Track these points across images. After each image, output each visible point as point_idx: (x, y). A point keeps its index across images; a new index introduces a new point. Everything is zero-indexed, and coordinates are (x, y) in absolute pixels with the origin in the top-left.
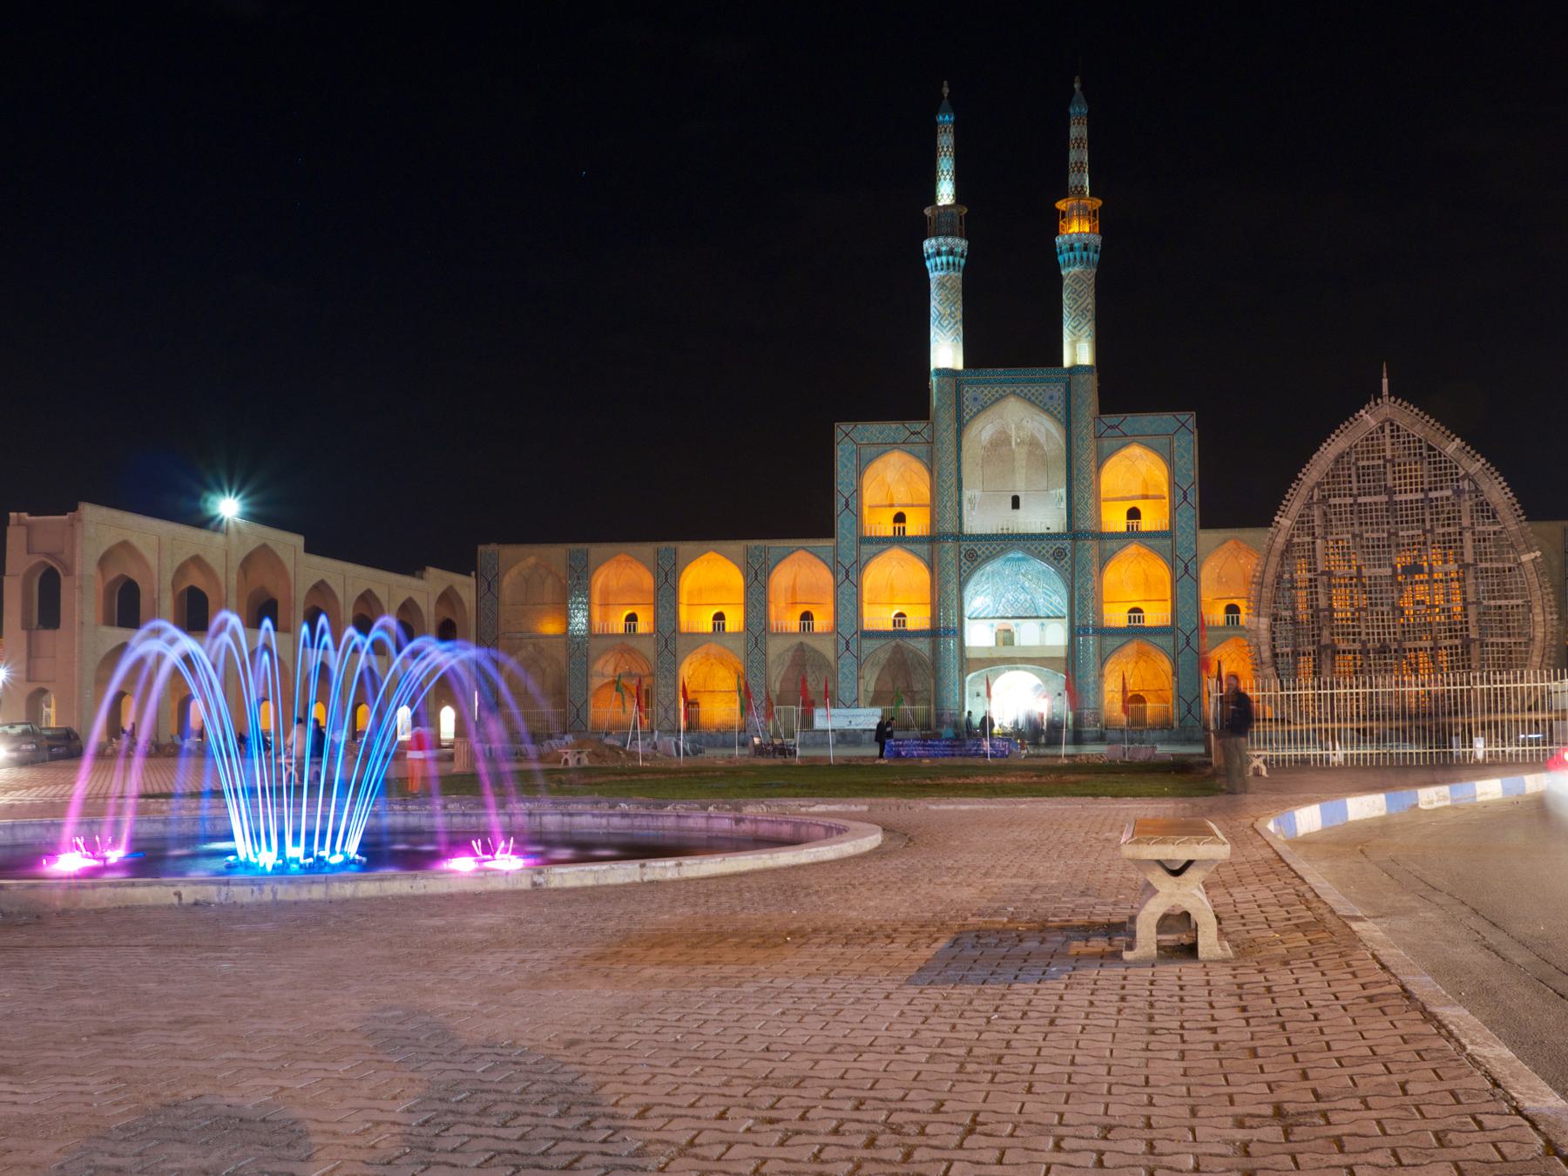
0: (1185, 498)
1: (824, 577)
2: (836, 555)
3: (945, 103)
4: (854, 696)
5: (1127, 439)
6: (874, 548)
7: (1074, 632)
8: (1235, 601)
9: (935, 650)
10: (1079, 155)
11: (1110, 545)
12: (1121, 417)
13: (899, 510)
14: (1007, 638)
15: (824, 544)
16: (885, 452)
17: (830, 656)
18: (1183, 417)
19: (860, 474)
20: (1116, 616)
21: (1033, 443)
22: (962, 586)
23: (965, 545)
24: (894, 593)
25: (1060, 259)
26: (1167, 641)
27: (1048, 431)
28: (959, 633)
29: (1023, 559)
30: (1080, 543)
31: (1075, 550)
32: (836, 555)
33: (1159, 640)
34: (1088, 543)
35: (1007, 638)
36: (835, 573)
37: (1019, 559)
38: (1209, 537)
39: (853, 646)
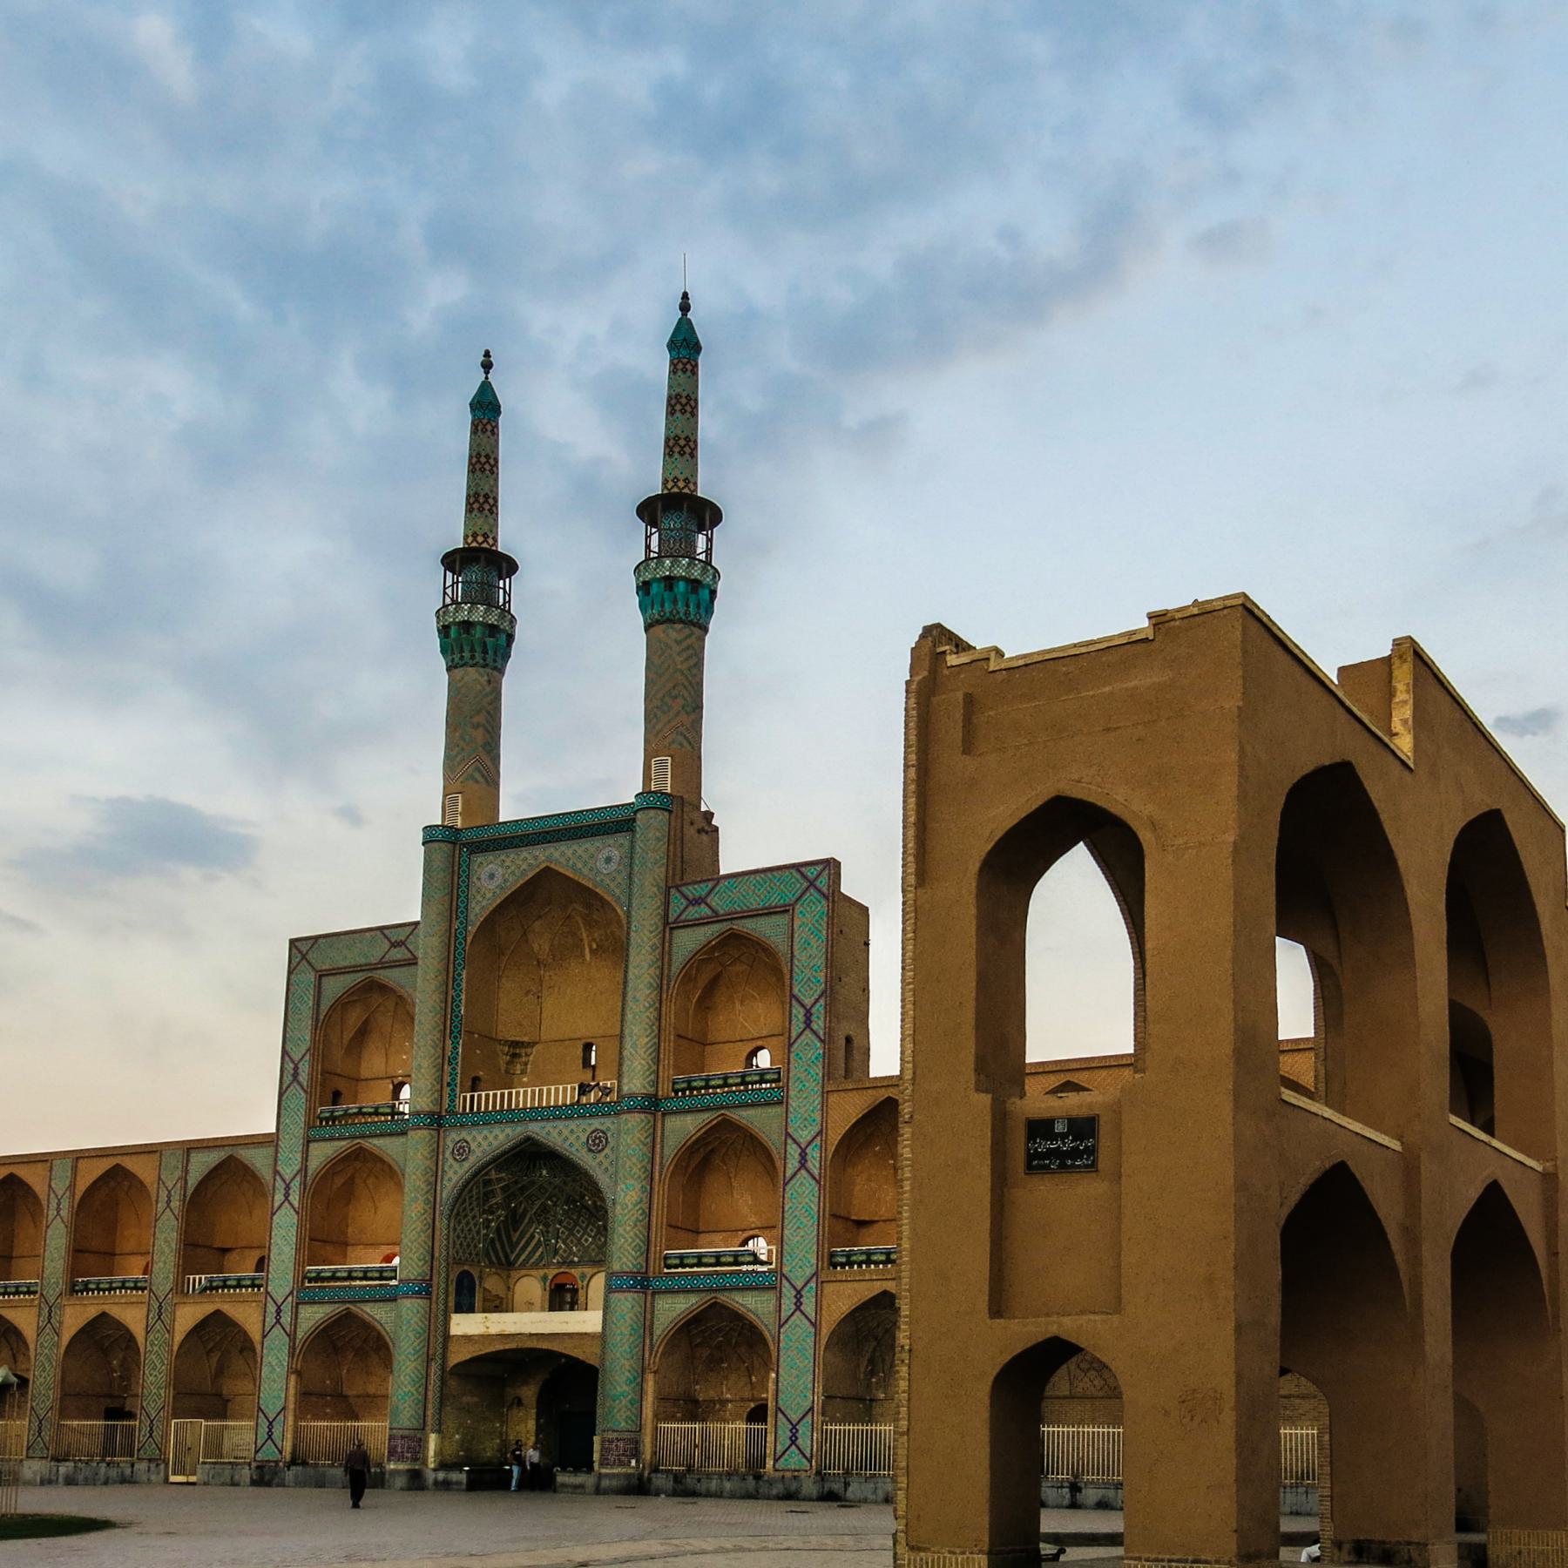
0: (808, 1023)
4: (280, 1405)
17: (255, 1333)
39: (286, 1319)
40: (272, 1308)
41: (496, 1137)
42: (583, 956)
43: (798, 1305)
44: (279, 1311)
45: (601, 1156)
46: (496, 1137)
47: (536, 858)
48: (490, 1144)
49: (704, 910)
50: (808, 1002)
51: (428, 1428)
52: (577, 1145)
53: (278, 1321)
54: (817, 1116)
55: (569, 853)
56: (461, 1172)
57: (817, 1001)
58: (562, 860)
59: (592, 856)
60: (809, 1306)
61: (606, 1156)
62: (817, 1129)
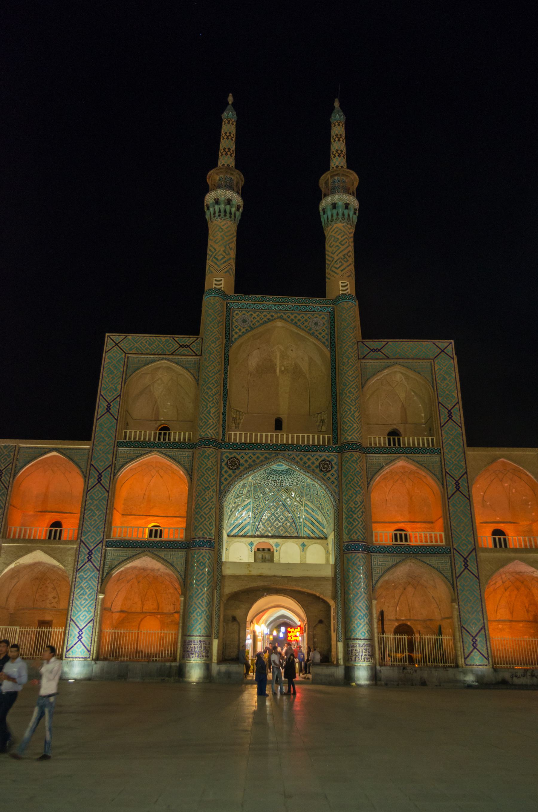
1: (76, 483)
3: (230, 107)
7: (344, 550)
8: (501, 526)
10: (338, 146)
11: (375, 458)
12: (383, 342)
14: (265, 555)
18: (443, 344)
20: (383, 535)
22: (221, 494)
25: (323, 218)
26: (443, 562)
28: (215, 545)
29: (287, 472)
30: (347, 454)
33: (433, 561)
34: (356, 455)
35: (265, 555)
36: (86, 477)
37: (282, 472)
38: (476, 454)
40: (85, 551)
41: (258, 458)
43: (466, 567)
45: (329, 475)
46: (258, 458)
47: (272, 316)
50: (449, 407)
51: (213, 636)
52: (313, 467)
54: (463, 463)
56: (233, 475)
58: (289, 320)
59: (306, 321)
60: (472, 567)
62: (462, 471)
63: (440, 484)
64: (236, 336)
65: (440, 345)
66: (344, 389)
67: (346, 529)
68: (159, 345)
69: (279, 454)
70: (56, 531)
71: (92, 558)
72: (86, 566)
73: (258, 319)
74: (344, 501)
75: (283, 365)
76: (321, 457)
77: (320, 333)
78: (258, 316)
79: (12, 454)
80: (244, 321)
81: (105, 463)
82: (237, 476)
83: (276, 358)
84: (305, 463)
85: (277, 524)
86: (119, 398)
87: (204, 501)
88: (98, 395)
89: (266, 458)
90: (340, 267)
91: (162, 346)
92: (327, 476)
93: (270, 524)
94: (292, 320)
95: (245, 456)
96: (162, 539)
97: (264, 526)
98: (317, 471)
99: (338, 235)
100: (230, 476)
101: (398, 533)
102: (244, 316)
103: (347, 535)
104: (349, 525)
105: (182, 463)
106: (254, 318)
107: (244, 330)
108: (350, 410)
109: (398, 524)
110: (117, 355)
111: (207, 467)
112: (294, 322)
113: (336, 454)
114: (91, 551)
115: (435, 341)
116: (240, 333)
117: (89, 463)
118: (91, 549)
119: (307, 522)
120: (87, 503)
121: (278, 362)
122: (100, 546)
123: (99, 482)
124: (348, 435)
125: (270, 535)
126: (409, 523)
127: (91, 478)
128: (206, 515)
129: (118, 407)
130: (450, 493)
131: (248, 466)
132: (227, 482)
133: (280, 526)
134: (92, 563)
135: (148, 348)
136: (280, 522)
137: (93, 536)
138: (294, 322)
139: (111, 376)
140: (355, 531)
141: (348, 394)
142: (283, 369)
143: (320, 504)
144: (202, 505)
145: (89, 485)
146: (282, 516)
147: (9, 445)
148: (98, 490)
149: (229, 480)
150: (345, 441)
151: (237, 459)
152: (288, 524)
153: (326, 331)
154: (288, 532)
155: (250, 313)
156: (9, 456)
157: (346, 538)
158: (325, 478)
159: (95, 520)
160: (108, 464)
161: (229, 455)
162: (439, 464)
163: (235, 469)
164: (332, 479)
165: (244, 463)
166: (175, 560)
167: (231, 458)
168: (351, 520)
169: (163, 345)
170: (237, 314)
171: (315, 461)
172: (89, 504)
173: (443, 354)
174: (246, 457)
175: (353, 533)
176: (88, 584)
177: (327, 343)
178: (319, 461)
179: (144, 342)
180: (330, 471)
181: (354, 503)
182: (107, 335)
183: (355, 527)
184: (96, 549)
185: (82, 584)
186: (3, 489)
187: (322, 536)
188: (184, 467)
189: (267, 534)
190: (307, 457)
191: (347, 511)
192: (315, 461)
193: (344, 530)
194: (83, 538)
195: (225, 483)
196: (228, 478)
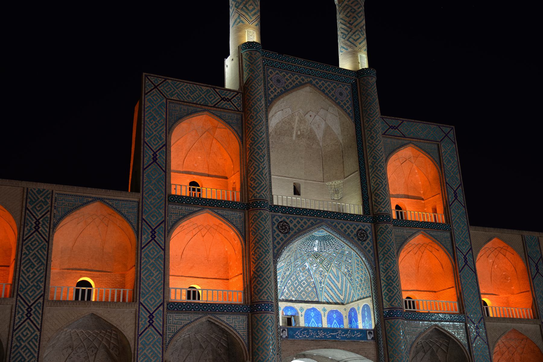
2: (140, 211)
5: (404, 140)
6: (184, 209)
9: (254, 330)
13: (196, 178)
15: (128, 198)
16: (196, 112)
17: (129, 333)
18: (447, 129)
19: (169, 131)
21: (311, 137)
23: (280, 217)
24: (200, 263)
27: (328, 127)
29: (323, 239)
30: (383, 226)
31: (374, 232)
32: (140, 211)
36: (138, 232)
38: (477, 233)
39: (158, 322)
41: (305, 223)
42: (292, 136)
44: (151, 316)
46: (305, 223)
47: (303, 80)
48: (302, 226)
49: (396, 132)
52: (352, 235)
53: (151, 324)
54: (468, 240)
55: (320, 83)
56: (285, 239)
57: (458, 188)
58: (318, 86)
61: (368, 244)
63: (451, 257)
64: (272, 96)
65: (444, 129)
66: (375, 163)
67: (386, 296)
68: (201, 95)
69: (323, 221)
70: (83, 291)
71: (153, 322)
72: (149, 331)
73: (291, 81)
74: (381, 269)
75: (300, 130)
76: (357, 226)
77: (345, 104)
78: (290, 77)
79: (49, 201)
80: (279, 81)
81: (157, 218)
82: (288, 240)
83: (294, 122)
84: (345, 231)
85: (300, 289)
86: (164, 147)
87: (266, 264)
88: (142, 141)
89: (312, 224)
90: (358, 39)
91: (203, 95)
92: (364, 245)
93: (293, 289)
94: (320, 87)
95: (293, 221)
96: (201, 301)
97: (288, 290)
98: (356, 239)
99: (355, 6)
100: (282, 239)
101: (408, 300)
102: (277, 75)
103: (389, 302)
104: (389, 292)
105: (234, 223)
106: (287, 80)
107: (279, 90)
108: (382, 183)
109: (409, 292)
110: (157, 100)
111: (265, 230)
112: (322, 89)
113: (370, 224)
114: (151, 314)
115: (441, 125)
116: (276, 93)
117: (140, 218)
118: (151, 312)
119: (327, 288)
120: (142, 261)
121: (295, 126)
122: (161, 308)
123: (153, 239)
124: (382, 207)
125: (294, 299)
126: (417, 292)
127: (144, 234)
128: (269, 278)
129: (164, 158)
130: (461, 266)
131: (297, 231)
132: (280, 245)
133: (302, 291)
134: (154, 327)
135: (189, 96)
136: (302, 287)
137: (153, 298)
138: (322, 89)
139: (154, 122)
140: (395, 299)
141: (379, 168)
142: (299, 133)
143: (349, 271)
144: (263, 269)
145: (143, 242)
146: (304, 281)
147: (44, 190)
148: (153, 248)
149: (281, 244)
150: (379, 212)
151: (287, 223)
152: (310, 289)
153: (350, 103)
154: (310, 297)
155: (283, 73)
156: (46, 203)
157: (386, 305)
158: (363, 247)
159: (153, 280)
160: (160, 219)
161: (278, 218)
162: (450, 239)
163: (286, 233)
164: (369, 248)
165: (294, 228)
166: (237, 324)
167: (281, 222)
168: (391, 288)
169: (205, 96)
170: (271, 73)
171: (353, 230)
172: (145, 261)
173: (446, 138)
174: (295, 222)
175: (393, 301)
176: (152, 351)
177: (351, 115)
178: (357, 230)
179: (185, 89)
180: (366, 240)
181: (393, 272)
182: (144, 74)
183: (396, 294)
184: (156, 312)
185: (145, 351)
186: (43, 242)
187: (338, 302)
188: (237, 228)
189: (291, 298)
190: (347, 225)
191: (386, 279)
192: (353, 230)
193: (384, 297)
194: (142, 301)
195: (278, 247)
196: (280, 241)
